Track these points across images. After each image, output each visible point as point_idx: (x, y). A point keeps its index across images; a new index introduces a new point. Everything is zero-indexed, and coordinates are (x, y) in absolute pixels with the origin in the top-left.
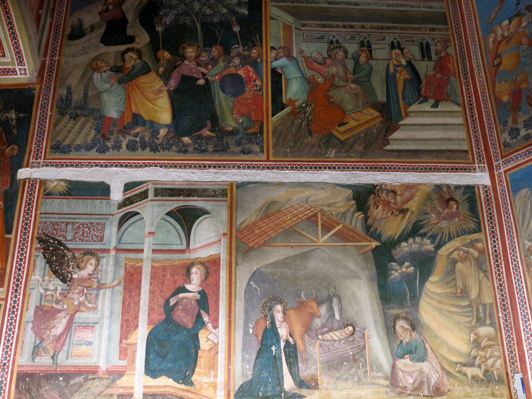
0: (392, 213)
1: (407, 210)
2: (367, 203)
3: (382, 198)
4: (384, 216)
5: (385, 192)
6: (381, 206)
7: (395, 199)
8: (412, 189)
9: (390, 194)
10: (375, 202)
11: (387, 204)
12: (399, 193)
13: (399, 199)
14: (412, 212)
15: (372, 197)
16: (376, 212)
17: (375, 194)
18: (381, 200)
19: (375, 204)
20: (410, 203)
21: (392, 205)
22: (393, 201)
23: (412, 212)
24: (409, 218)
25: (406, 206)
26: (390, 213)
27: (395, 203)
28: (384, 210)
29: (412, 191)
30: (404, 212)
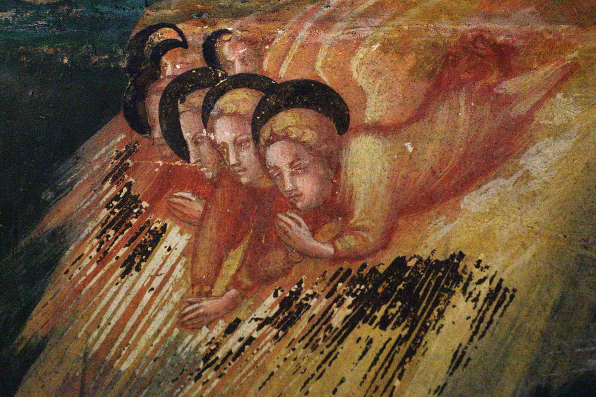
0: (290, 310)
1: (448, 272)
2: (42, 209)
3: (199, 156)
4: (197, 341)
5: (241, 100)
6: (176, 239)
7: (332, 164)
8: (508, 73)
9: (286, 120)
10: (128, 203)
11: (249, 214)
12: (375, 108)
13: (367, 162)
14: (498, 296)
15: (110, 143)
16: (117, 296)
17: (140, 125)
18: (195, 181)
19: (118, 223)
20: (474, 202)
21: (298, 230)
22: (306, 187)
23: (498, 296)
24: (458, 359)
25: (433, 238)
26: (268, 305)
27: (331, 210)
28: (201, 286)
29: (510, 86)
30: (411, 300)
